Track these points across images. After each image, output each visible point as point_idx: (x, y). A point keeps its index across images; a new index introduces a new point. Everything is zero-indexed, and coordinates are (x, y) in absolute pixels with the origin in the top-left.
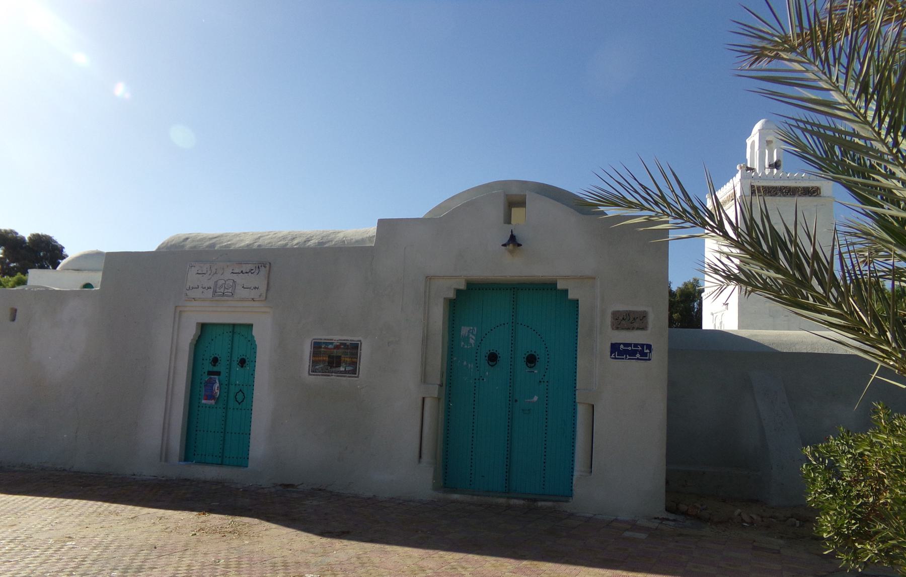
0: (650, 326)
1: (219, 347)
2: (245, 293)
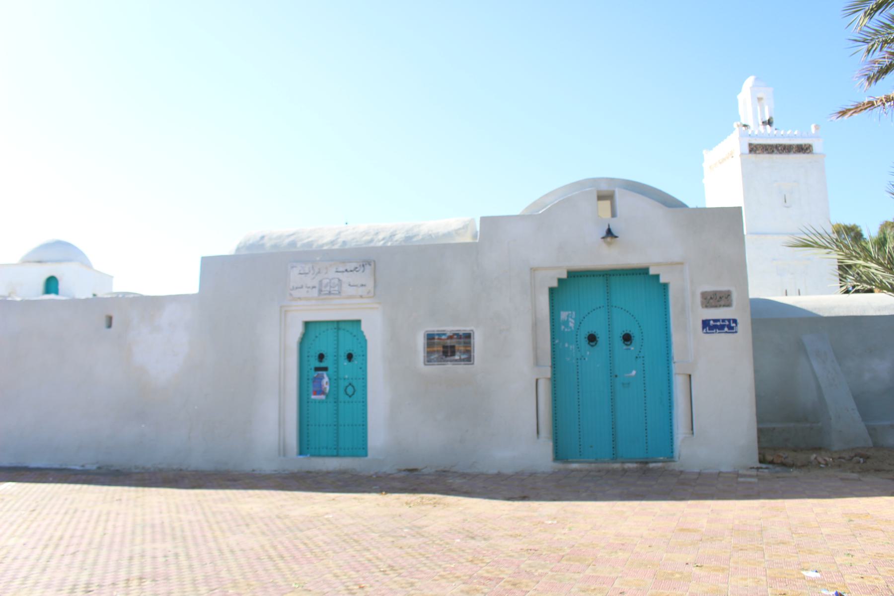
0: (734, 303)
1: (325, 343)
2: (351, 291)
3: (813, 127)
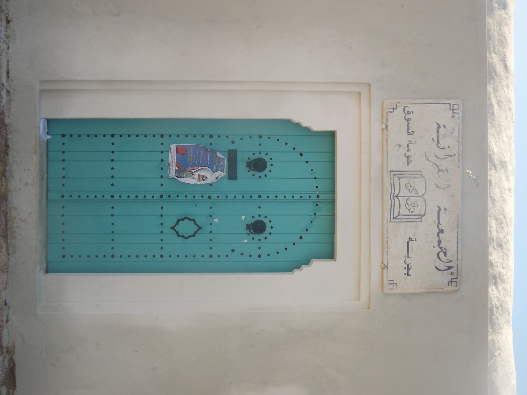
1: (288, 172)
2: (397, 246)
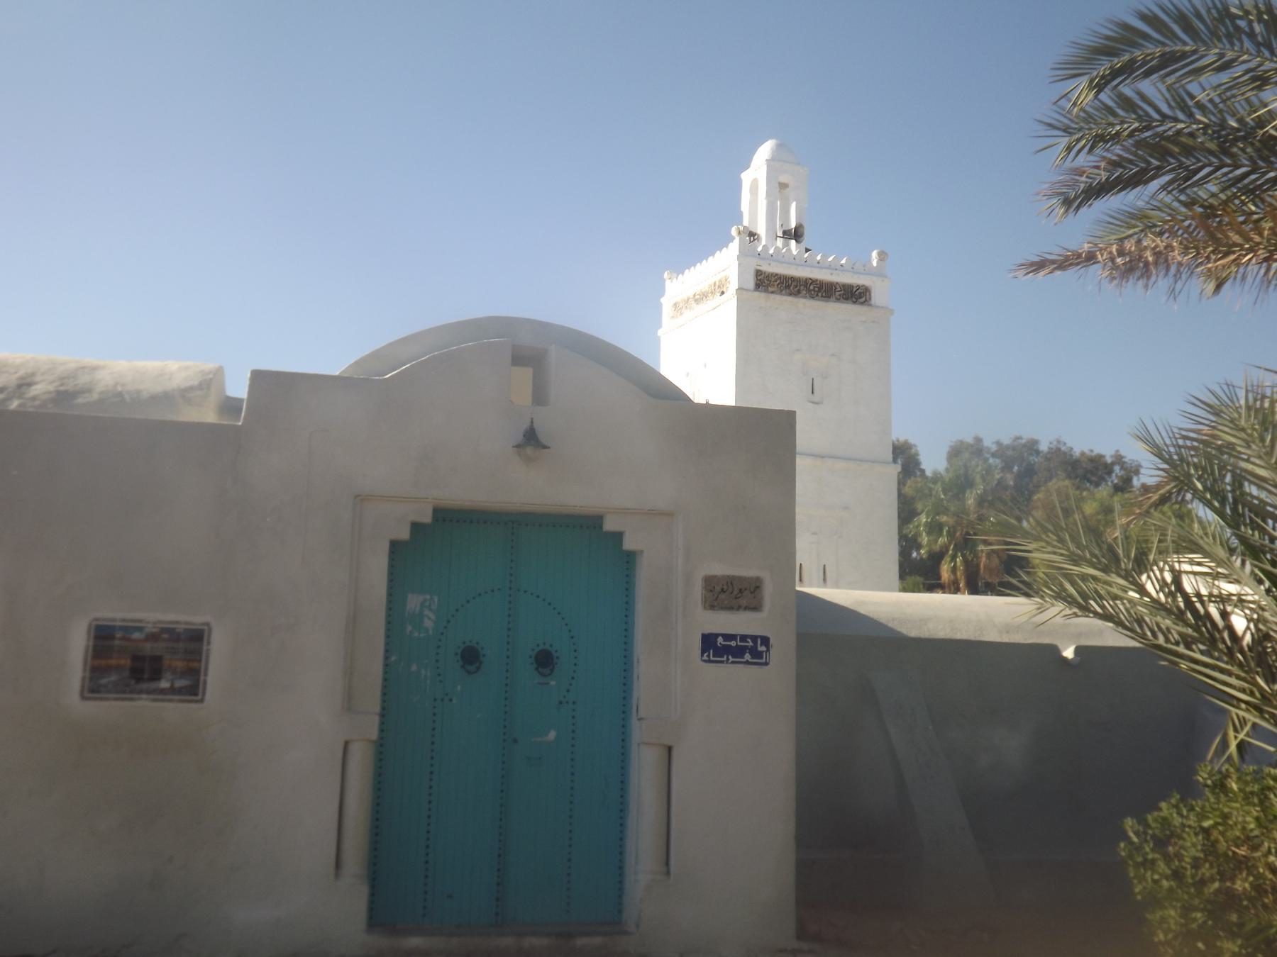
0: (767, 603)
3: (874, 254)
